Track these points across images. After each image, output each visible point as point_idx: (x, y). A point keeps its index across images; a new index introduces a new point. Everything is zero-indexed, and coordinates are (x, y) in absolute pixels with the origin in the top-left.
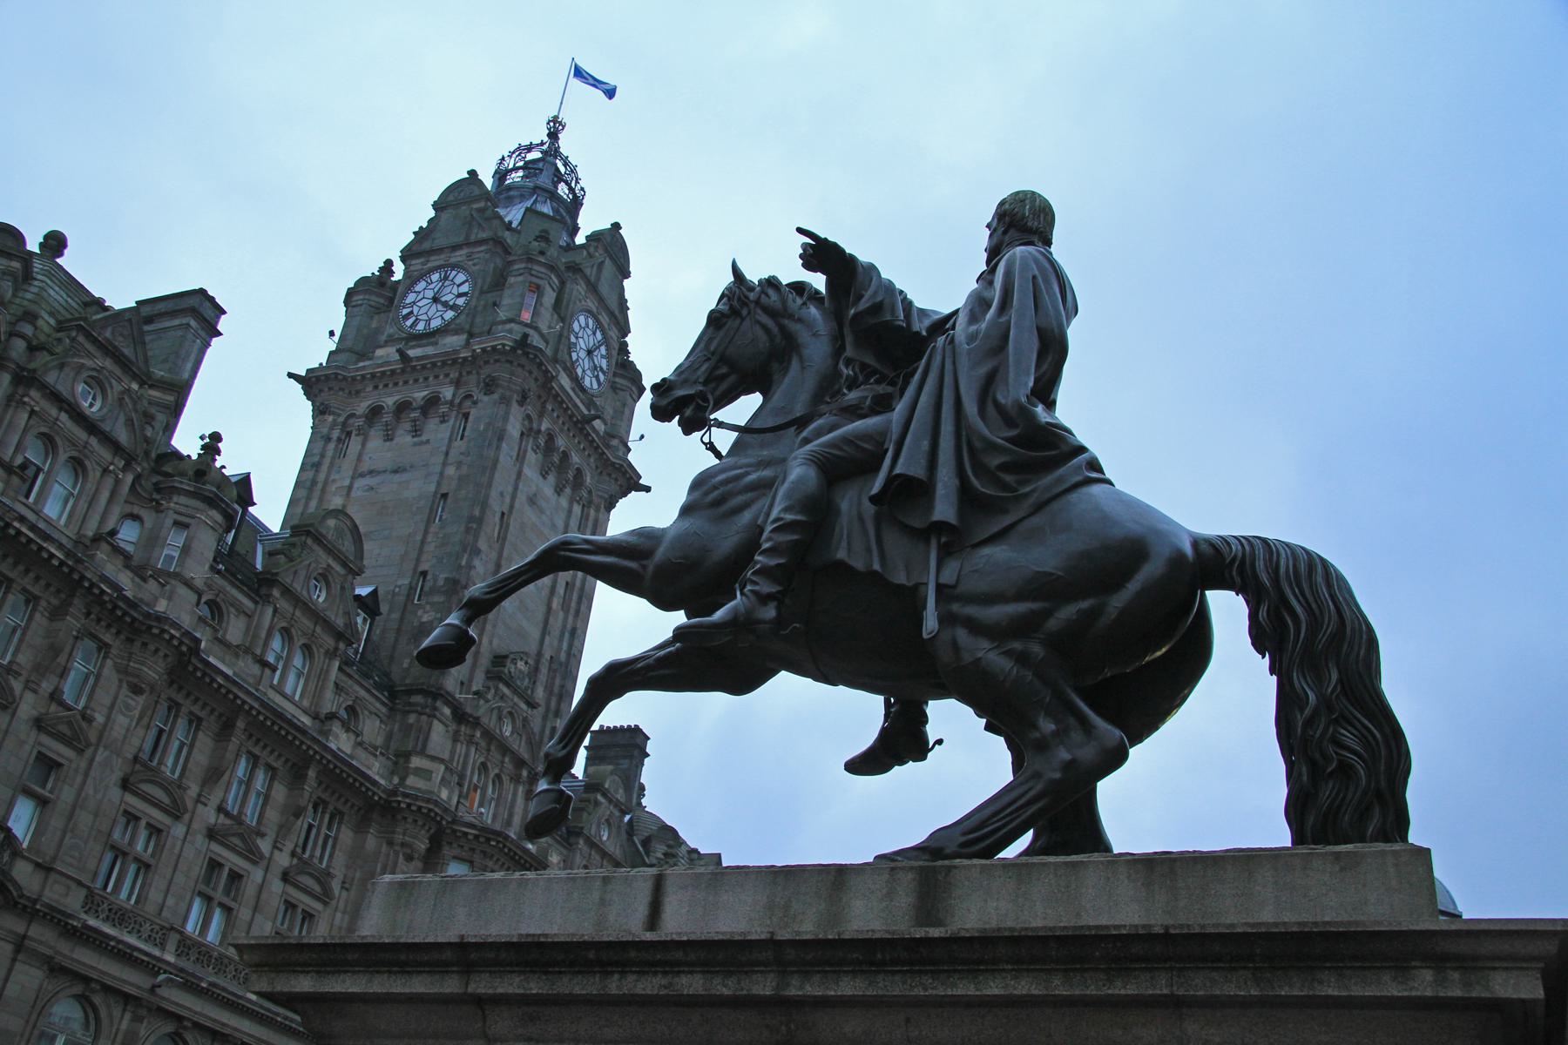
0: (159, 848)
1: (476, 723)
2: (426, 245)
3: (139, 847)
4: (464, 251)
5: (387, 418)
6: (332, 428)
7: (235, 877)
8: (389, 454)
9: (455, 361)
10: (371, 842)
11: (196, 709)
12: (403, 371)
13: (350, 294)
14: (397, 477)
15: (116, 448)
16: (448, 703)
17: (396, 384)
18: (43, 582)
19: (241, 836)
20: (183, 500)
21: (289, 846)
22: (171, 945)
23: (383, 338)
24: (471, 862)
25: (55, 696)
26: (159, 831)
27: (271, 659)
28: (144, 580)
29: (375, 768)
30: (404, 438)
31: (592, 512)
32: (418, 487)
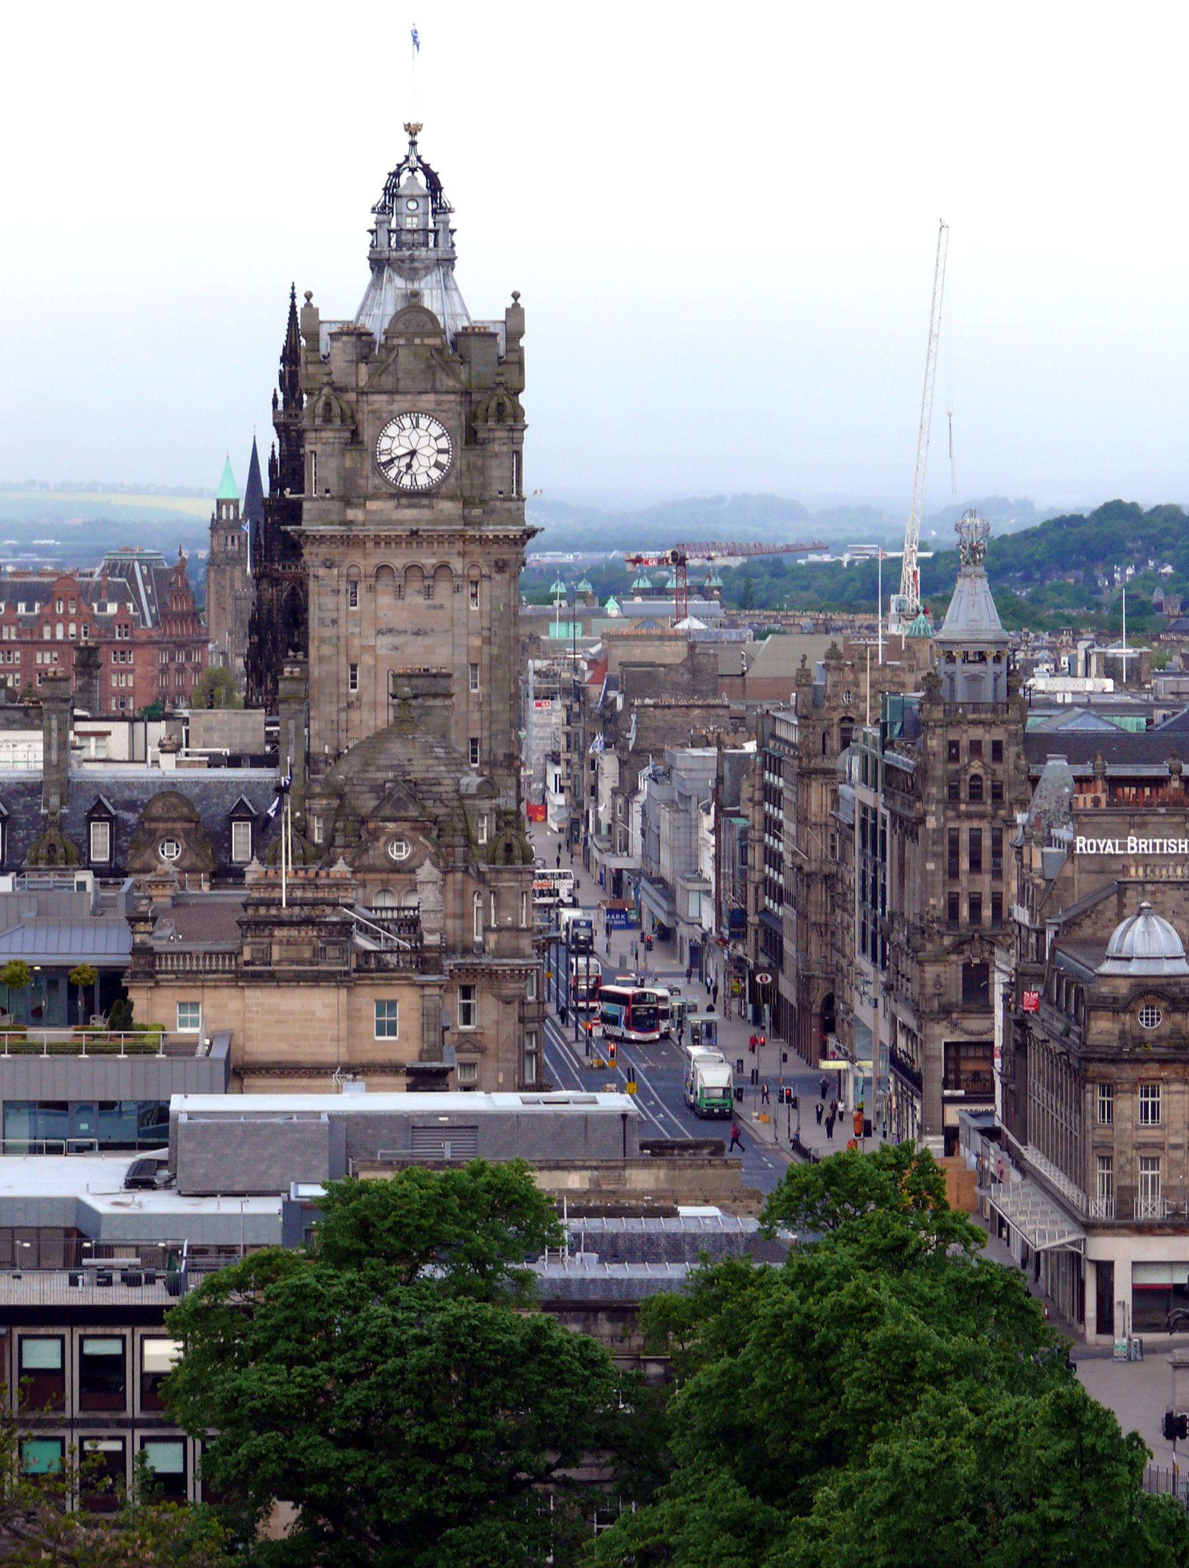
4: (432, 397)
8: (405, 614)
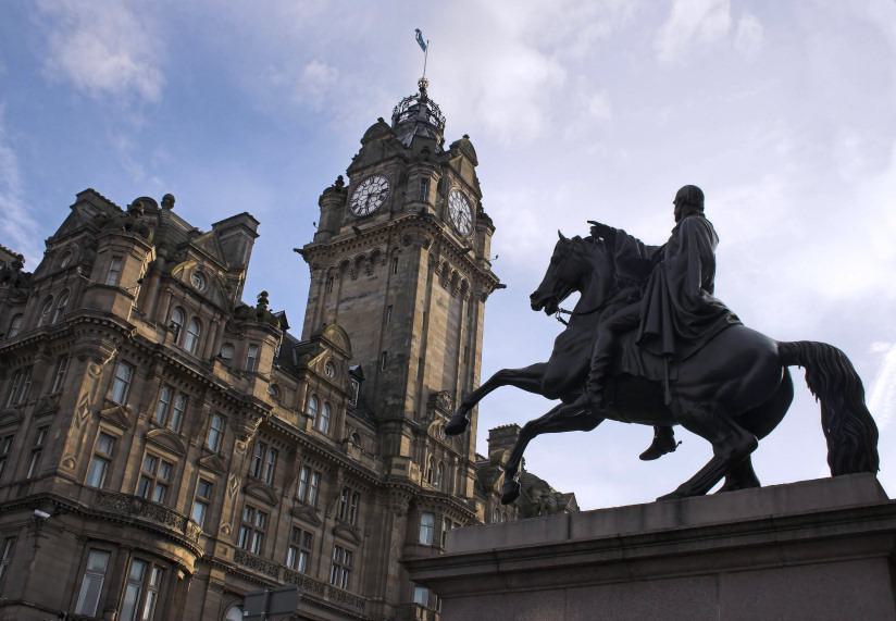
0: (267, 523)
1: (425, 434)
2: (360, 165)
3: (257, 524)
4: (382, 165)
5: (352, 267)
6: (322, 277)
7: (309, 535)
8: (356, 288)
9: (386, 229)
10: (377, 509)
11: (275, 446)
12: (357, 238)
13: (321, 198)
14: (363, 300)
15: (216, 308)
16: (408, 425)
17: (354, 247)
18: (190, 387)
19: (308, 513)
20: (253, 331)
21: (333, 514)
22: (281, 576)
23: (343, 222)
24: (434, 514)
25: (203, 448)
26: (266, 514)
27: (310, 412)
28: (239, 379)
29: (374, 466)
30: (363, 277)
31: (474, 305)
32: (375, 304)
